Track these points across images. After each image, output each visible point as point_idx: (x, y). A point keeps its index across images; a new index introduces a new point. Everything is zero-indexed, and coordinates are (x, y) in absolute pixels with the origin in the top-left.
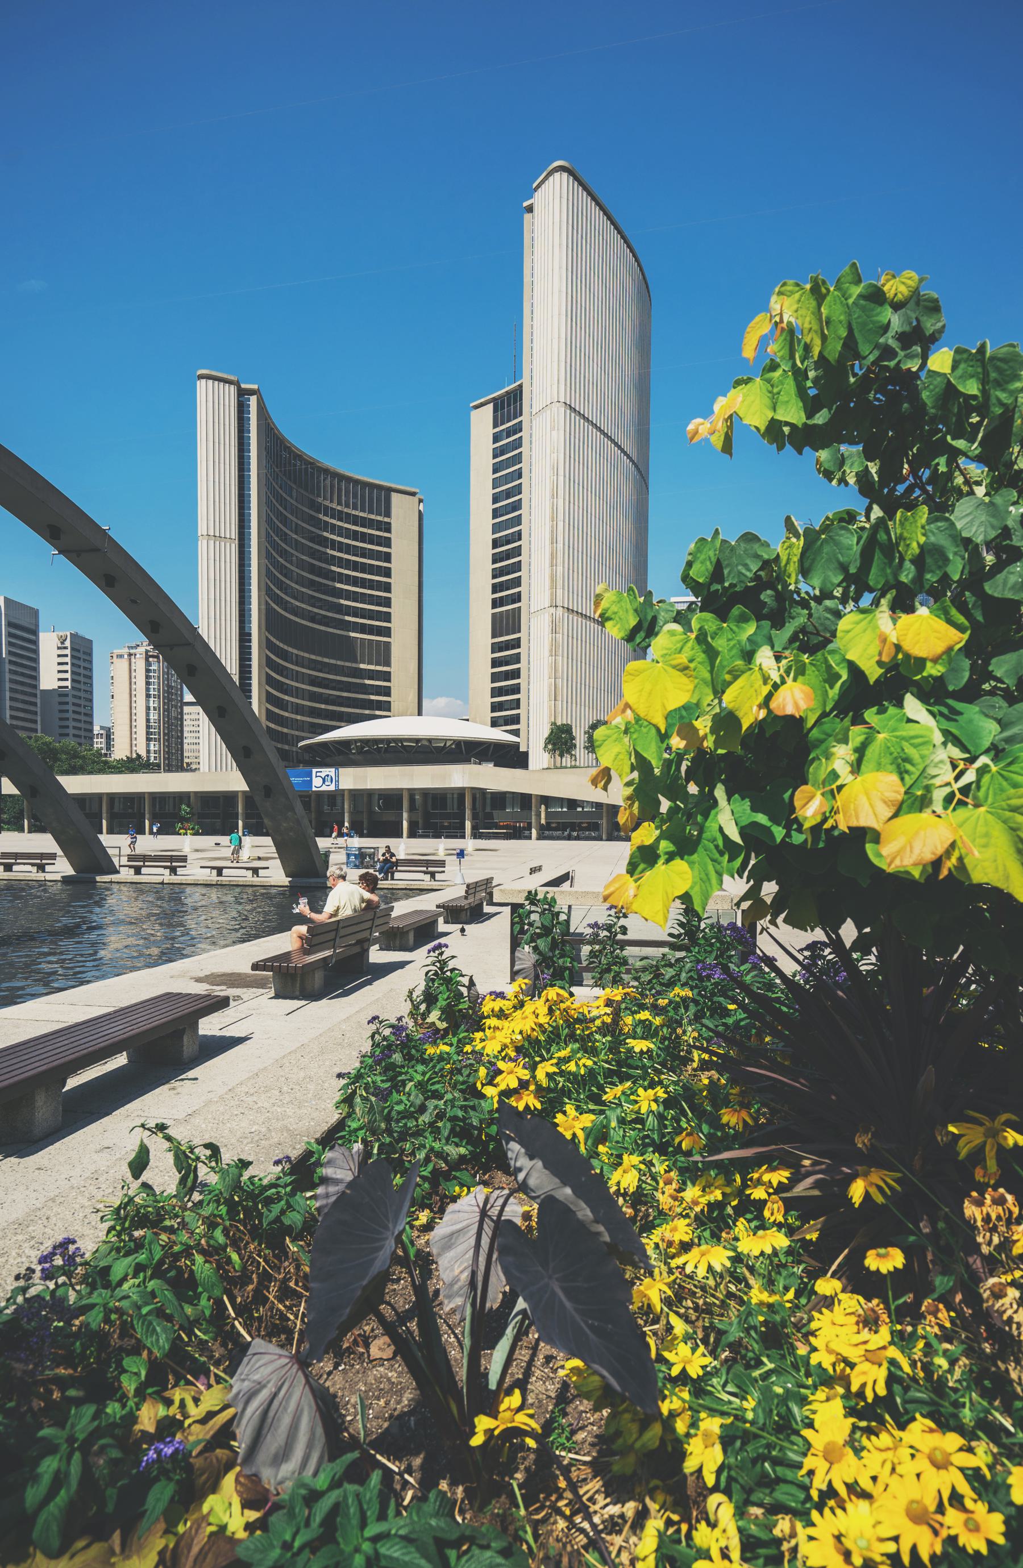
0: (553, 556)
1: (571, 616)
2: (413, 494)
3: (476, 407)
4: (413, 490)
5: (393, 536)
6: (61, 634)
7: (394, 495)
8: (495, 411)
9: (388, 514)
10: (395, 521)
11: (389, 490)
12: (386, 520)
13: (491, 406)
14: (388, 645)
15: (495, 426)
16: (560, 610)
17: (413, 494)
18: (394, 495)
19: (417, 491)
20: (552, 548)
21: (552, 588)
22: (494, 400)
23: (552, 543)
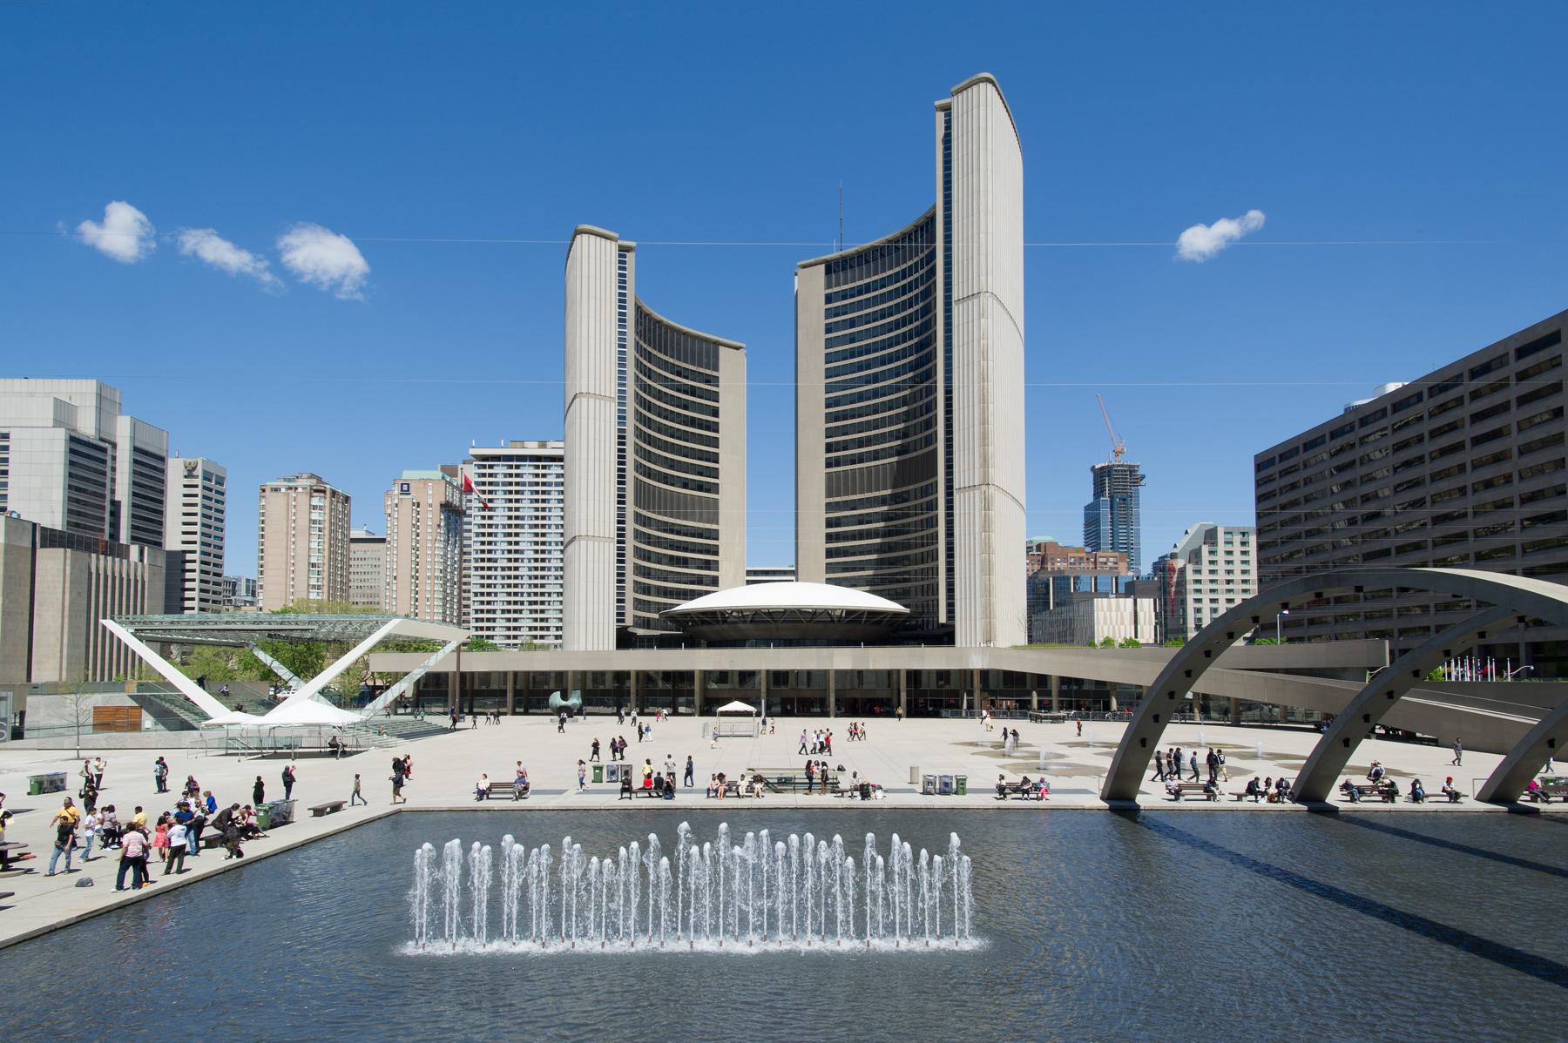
3: (805, 267)
4: (739, 344)
6: (189, 460)
7: (721, 348)
8: (828, 271)
10: (724, 373)
11: (717, 344)
12: (714, 373)
13: (823, 267)
14: (716, 501)
15: (828, 286)
18: (721, 348)
19: (744, 345)
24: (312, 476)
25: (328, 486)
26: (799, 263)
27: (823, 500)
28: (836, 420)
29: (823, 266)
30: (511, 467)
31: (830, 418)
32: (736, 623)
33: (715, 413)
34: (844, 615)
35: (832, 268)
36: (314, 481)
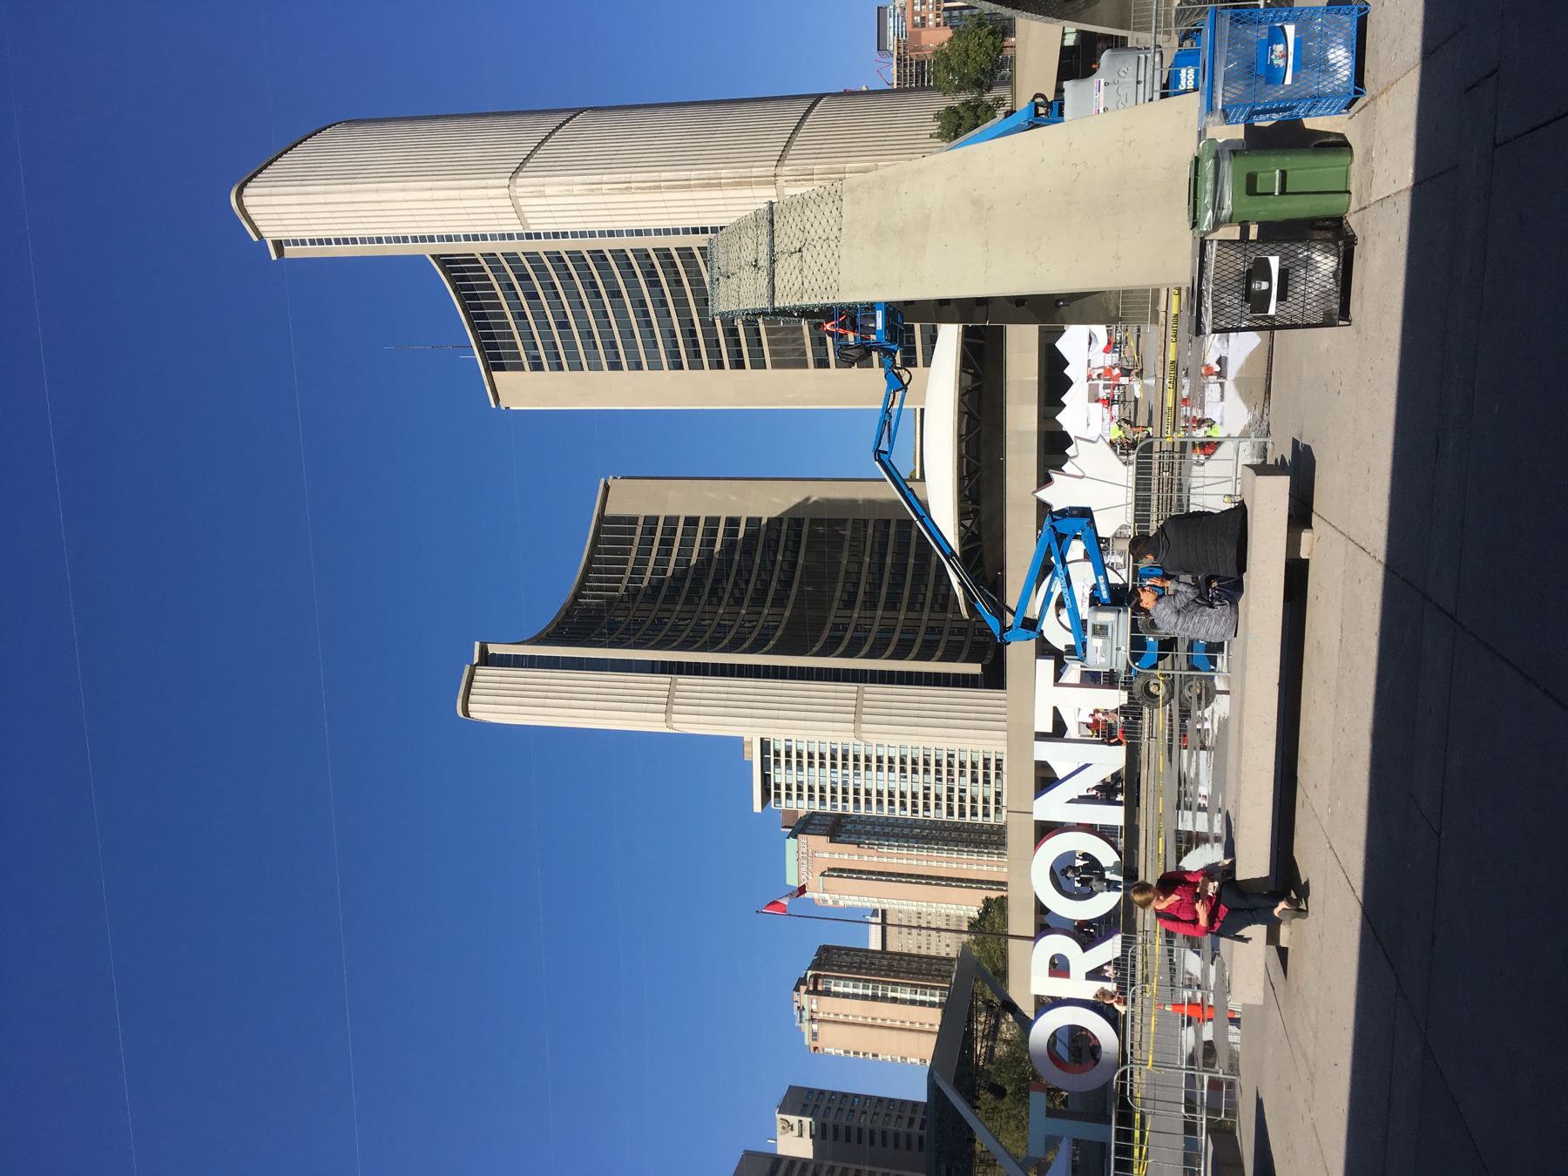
0: (707, 185)
1: (788, 157)
2: (607, 488)
5: (662, 513)
8: (501, 368)
9: (634, 520)
11: (602, 518)
12: (641, 522)
15: (520, 368)
16: (785, 170)
17: (607, 488)
18: (611, 511)
19: (603, 480)
20: (696, 186)
21: (750, 184)
22: (487, 370)
23: (689, 186)
24: (797, 989)
25: (810, 973)
26: (493, 406)
27: (812, 372)
28: (698, 354)
29: (493, 373)
30: (777, 762)
31: (696, 364)
32: (979, 522)
33: (692, 521)
34: (972, 371)
35: (496, 363)
36: (803, 989)
